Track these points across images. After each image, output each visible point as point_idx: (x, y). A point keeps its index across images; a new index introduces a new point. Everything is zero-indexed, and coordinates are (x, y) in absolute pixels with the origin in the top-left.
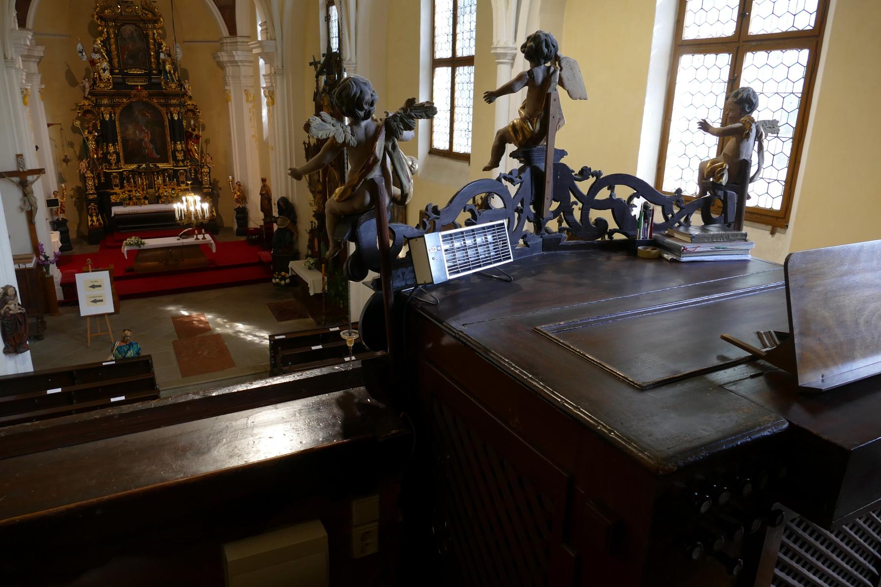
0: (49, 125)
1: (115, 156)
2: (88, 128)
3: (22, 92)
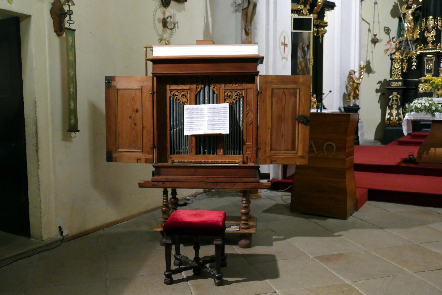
1: (433, 33)
2: (407, 3)
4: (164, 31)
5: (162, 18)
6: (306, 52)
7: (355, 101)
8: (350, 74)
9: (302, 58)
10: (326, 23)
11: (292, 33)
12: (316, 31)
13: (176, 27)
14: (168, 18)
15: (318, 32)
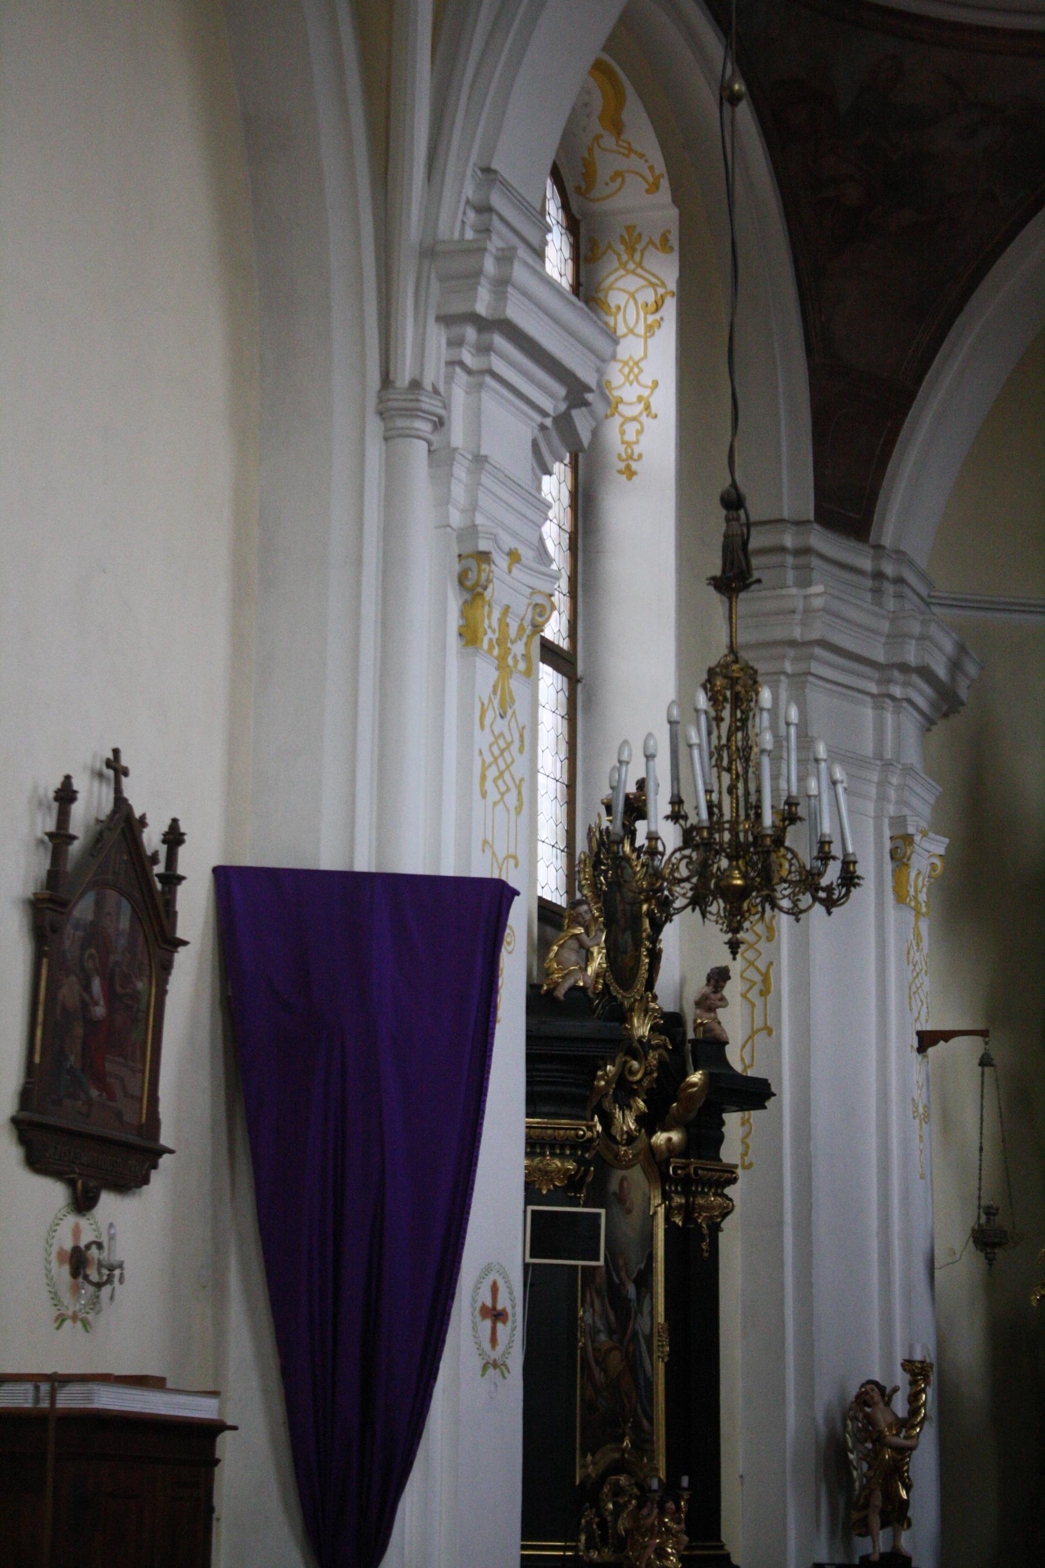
0: (926, 1040)
3: (462, 579)
4: (76, 1290)
5: (68, 1246)
6: (634, 1305)
7: (896, 1537)
8: (863, 1399)
9: (611, 1332)
10: (731, 1169)
11: (526, 1266)
12: (680, 1207)
13: (116, 1280)
14: (88, 1247)
15: (688, 1211)
